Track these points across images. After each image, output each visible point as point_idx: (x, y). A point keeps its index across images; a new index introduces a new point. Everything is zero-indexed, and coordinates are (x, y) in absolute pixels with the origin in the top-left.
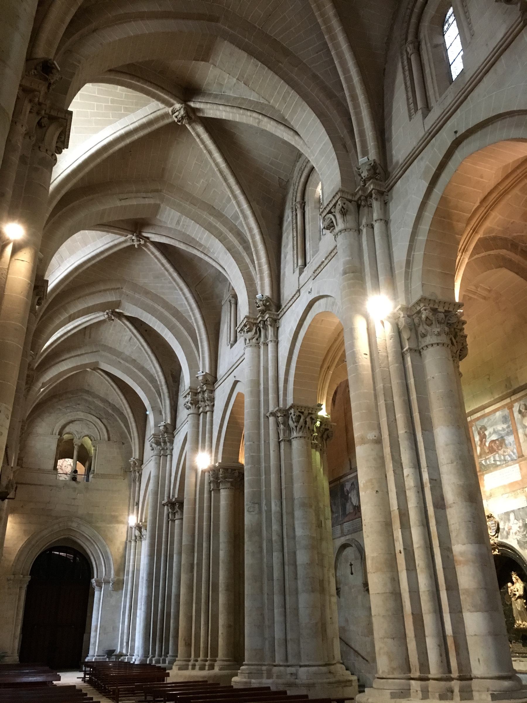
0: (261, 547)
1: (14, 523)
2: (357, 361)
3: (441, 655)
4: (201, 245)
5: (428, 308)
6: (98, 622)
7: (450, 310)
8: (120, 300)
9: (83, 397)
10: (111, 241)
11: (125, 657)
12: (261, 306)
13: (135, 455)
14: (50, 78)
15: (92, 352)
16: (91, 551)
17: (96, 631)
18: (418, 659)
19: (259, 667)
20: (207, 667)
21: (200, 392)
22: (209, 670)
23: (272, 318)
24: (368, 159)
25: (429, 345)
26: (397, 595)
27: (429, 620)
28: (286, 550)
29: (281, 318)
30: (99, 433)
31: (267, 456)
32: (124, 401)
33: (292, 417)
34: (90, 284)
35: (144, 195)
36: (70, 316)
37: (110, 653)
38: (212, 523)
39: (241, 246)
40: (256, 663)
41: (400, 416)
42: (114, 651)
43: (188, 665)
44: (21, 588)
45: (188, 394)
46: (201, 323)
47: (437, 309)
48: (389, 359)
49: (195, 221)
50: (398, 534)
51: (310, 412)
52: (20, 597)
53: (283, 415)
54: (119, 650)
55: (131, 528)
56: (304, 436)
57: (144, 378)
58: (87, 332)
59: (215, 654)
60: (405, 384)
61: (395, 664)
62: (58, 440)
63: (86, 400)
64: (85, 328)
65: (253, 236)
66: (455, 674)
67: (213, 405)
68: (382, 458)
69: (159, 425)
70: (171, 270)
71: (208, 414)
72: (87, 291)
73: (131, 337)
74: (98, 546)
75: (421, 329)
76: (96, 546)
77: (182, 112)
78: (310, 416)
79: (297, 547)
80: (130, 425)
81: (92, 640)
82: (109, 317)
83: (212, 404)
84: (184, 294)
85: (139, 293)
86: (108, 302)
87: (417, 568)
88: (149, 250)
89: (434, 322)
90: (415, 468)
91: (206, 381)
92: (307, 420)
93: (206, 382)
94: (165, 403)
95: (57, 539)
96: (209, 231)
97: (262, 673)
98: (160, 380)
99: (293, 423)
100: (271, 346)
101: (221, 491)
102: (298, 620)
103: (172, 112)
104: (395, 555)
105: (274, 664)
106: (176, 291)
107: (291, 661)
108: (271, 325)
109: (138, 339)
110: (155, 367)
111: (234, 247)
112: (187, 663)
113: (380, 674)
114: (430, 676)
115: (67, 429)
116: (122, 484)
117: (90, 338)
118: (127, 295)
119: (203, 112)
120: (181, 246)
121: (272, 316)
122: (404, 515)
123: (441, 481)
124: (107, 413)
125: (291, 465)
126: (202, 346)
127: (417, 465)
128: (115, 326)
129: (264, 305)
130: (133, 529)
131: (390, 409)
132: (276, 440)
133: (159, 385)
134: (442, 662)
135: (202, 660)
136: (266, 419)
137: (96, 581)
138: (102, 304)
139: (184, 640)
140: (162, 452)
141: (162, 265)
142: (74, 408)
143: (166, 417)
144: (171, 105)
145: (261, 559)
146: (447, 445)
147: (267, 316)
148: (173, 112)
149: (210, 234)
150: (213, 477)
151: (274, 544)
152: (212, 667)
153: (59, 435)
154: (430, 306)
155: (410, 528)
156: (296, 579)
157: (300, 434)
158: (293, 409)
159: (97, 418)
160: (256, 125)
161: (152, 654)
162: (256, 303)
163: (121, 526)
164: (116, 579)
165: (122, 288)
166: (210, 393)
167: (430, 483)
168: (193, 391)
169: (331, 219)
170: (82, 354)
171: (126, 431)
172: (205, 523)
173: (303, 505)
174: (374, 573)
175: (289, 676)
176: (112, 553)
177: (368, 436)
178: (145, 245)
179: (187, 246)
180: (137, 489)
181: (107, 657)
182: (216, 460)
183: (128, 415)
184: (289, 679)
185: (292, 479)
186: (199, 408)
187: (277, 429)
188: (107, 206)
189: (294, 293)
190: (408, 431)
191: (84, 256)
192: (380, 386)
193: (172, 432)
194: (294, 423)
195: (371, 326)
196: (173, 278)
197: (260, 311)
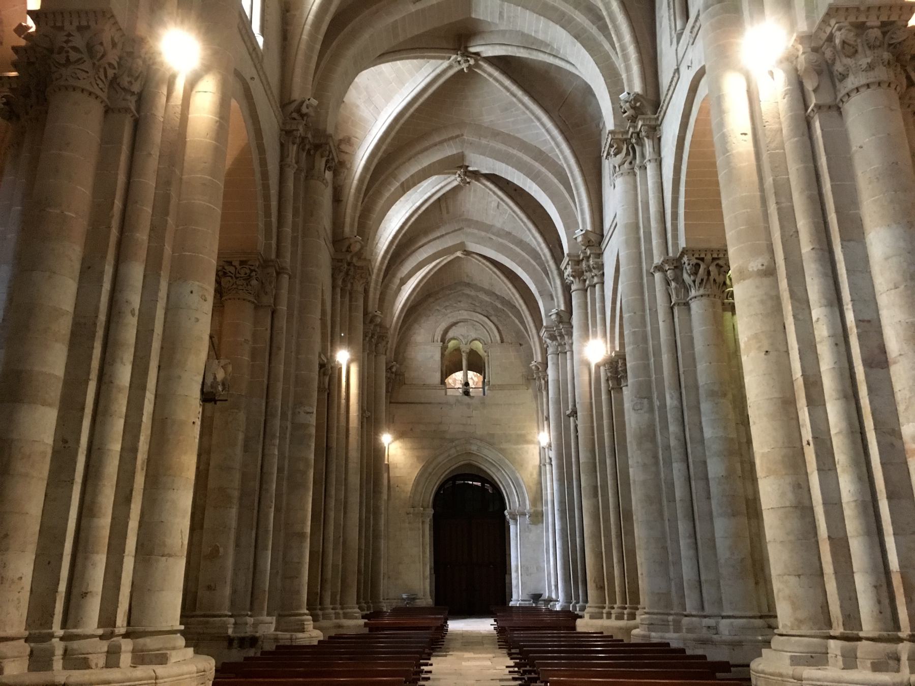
0: (656, 457)
1: (406, 449)
2: (729, 148)
3: (879, 602)
4: (547, 45)
5: (846, 24)
7: (892, 19)
8: (463, 152)
9: (464, 292)
10: (433, 71)
11: (555, 603)
12: (629, 110)
13: (537, 358)
15: (455, 231)
16: (498, 478)
17: (517, 571)
18: (841, 607)
19: (665, 617)
20: (626, 616)
21: (583, 260)
22: (628, 620)
23: (647, 125)
25: (852, 90)
26: (804, 510)
27: (857, 547)
28: (690, 460)
29: (661, 124)
30: (489, 334)
31: (656, 331)
32: (514, 290)
33: (686, 268)
34: (425, 136)
36: (402, 185)
37: (537, 597)
38: (615, 433)
39: (594, 27)
40: (661, 611)
41: (803, 224)
42: (540, 595)
43: (602, 613)
44: (423, 522)
45: (568, 264)
46: (572, 161)
47: (864, 23)
48: (784, 132)
49: (523, 7)
50: (804, 415)
51: (715, 256)
52: (423, 531)
53: (673, 268)
54: (547, 595)
55: (544, 448)
56: (707, 293)
57: (524, 254)
58: (443, 205)
59: (635, 600)
60: (813, 169)
61: (802, 614)
62: (442, 349)
63: (468, 296)
64: (439, 199)
66: (905, 632)
67: (603, 274)
68: (778, 299)
69: (550, 314)
70: (520, 93)
71: (597, 287)
72: (418, 148)
73: (499, 203)
74: (506, 472)
75: (838, 68)
76: (503, 471)
78: (715, 263)
79: (707, 453)
80: (526, 321)
81: (514, 582)
82: (462, 180)
83: (601, 272)
85: (486, 137)
86: (448, 157)
87: (837, 466)
88: (485, 71)
89: (860, 49)
90: (831, 306)
91: (589, 242)
92: (711, 269)
93: (588, 243)
94: (555, 283)
95: (456, 466)
96: (544, 16)
97: (669, 625)
98: (544, 255)
99: (688, 277)
101: (624, 388)
102: (715, 555)
104: (802, 448)
105: (685, 613)
106: (534, 124)
107: (708, 610)
108: (648, 137)
109: (507, 204)
110: (535, 238)
111: (584, 30)
112: (601, 610)
113: (781, 630)
114: (861, 634)
115: (450, 334)
116: (527, 395)
117: (448, 213)
118: (471, 143)
121: (648, 123)
122: (813, 384)
123: (880, 321)
124: (496, 309)
125: (692, 339)
126: (578, 194)
127: (835, 301)
128: (475, 191)
129: (634, 108)
130: (546, 450)
131: (787, 217)
132: (667, 305)
133: (545, 261)
134: (881, 613)
135: (619, 608)
136: (651, 278)
137: (510, 514)
138: (439, 162)
139: (594, 581)
140: (559, 349)
142: (455, 307)
143: (558, 302)
145: (657, 474)
146: (887, 259)
147: (640, 123)
149: (546, 20)
150: (610, 372)
151: (673, 452)
152: (632, 616)
154: (848, 20)
155: (825, 405)
156: (709, 498)
157: (702, 291)
158: (686, 256)
159: (484, 316)
161: (575, 599)
162: (621, 107)
163: (531, 446)
164: (532, 511)
165: (462, 135)
166: (596, 258)
167: (857, 327)
168: (573, 258)
170: (442, 236)
171: (522, 328)
172: (606, 434)
173: (712, 394)
174: (765, 477)
175: (704, 630)
176: (524, 479)
177: (750, 267)
178: (477, 65)
179: (529, 51)
180: (545, 400)
181: (533, 602)
182: (613, 348)
183: (521, 307)
184: (705, 634)
185: (694, 359)
186: (585, 281)
187: (667, 289)
188: (397, 17)
189: (672, 75)
190: (817, 247)
191: (403, 101)
192: (769, 181)
193: (568, 321)
195: (753, 86)
196: (523, 104)
197: (628, 118)
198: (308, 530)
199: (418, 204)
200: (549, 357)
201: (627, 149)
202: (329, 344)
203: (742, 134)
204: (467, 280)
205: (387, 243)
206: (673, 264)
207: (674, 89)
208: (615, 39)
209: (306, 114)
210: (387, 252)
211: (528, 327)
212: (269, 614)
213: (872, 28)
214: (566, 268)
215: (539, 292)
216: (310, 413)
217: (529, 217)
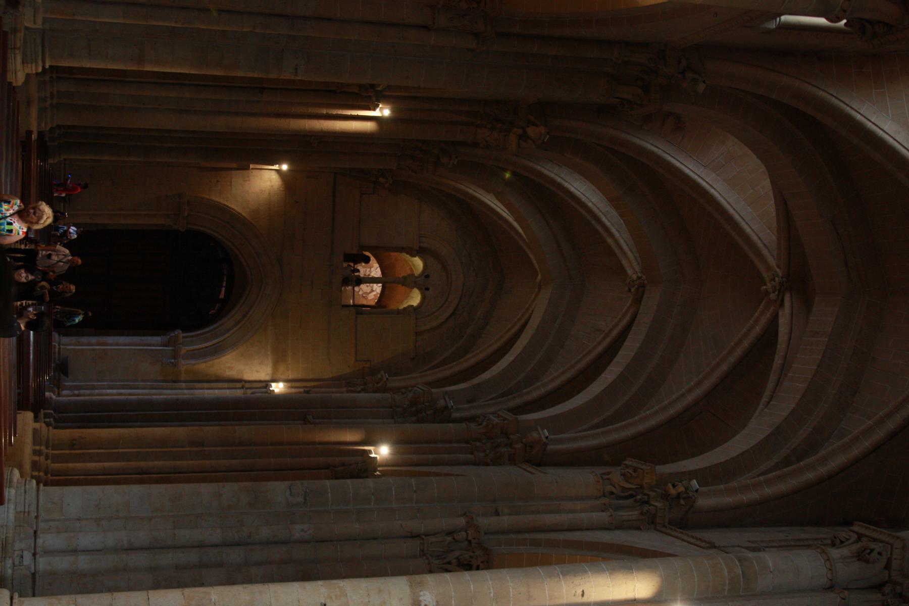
6: (111, 345)
10: (765, 245)
17: (99, 344)
29: (661, 532)
42: (66, 374)
45: (504, 419)
46: (641, 428)
67: (487, 464)
69: (447, 399)
73: (604, 331)
81: (84, 340)
84: (690, 390)
113: (16, 599)
120: (777, 362)
129: (678, 496)
130: (264, 390)
140: (398, 409)
141: (739, 342)
147: (659, 505)
153: (420, 247)
159: (455, 310)
169: (848, 540)
194: (456, 559)
198: (148, 68)
199: (604, 219)
200: (388, 395)
201: (631, 489)
202: (403, 94)
203: (583, 591)
206: (474, 539)
207: (692, 544)
208: (770, 475)
211: (437, 370)
212: (45, 20)
215: (479, 384)
216: (296, 72)
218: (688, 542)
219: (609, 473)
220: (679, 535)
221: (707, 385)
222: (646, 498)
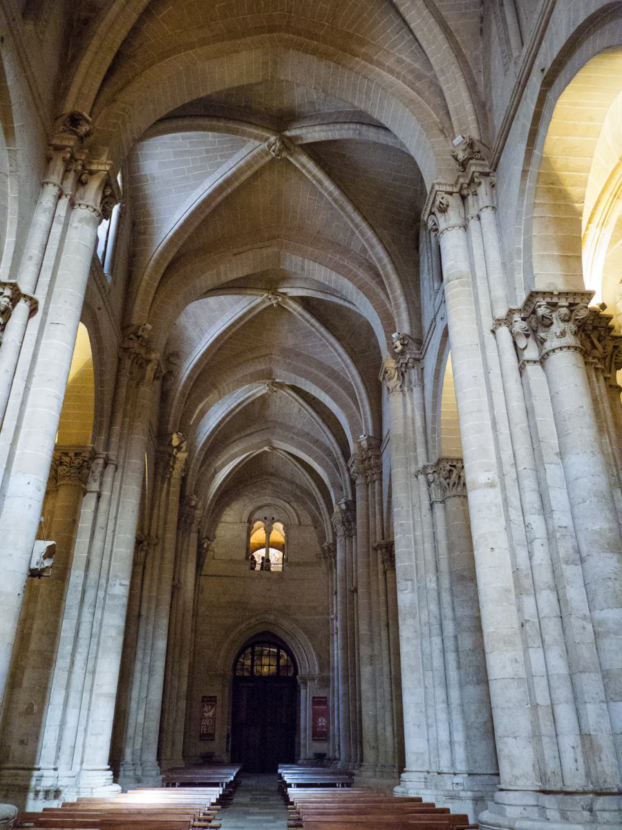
7: (576, 302)
10: (249, 304)
14: (79, 131)
17: (305, 731)
21: (365, 460)
24: (464, 138)
32: (311, 480)
35: (261, 245)
42: (324, 755)
46: (358, 379)
47: (557, 303)
65: (384, 267)
67: (382, 472)
71: (377, 483)
77: (278, 144)
81: (302, 742)
82: (270, 389)
84: (336, 351)
88: (290, 306)
89: (555, 321)
100: (417, 390)
103: (268, 146)
109: (306, 410)
110: (329, 439)
119: (302, 139)
120: (320, 296)
121: (413, 357)
126: (363, 406)
141: (308, 322)
142: (261, 493)
144: (267, 139)
147: (408, 356)
148: (270, 146)
160: (358, 137)
186: (367, 477)
196: (321, 333)
199: (232, 407)
200: (338, 540)
204: (272, 470)
205: (205, 438)
209: (141, 336)
210: (204, 445)
213: (563, 307)
214: (351, 466)
217: (324, 421)
218: (432, 335)
219: (388, 389)
220: (427, 343)
221: (332, 340)
222: (404, 365)
